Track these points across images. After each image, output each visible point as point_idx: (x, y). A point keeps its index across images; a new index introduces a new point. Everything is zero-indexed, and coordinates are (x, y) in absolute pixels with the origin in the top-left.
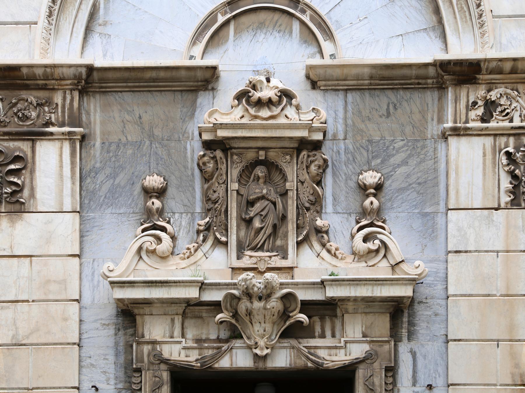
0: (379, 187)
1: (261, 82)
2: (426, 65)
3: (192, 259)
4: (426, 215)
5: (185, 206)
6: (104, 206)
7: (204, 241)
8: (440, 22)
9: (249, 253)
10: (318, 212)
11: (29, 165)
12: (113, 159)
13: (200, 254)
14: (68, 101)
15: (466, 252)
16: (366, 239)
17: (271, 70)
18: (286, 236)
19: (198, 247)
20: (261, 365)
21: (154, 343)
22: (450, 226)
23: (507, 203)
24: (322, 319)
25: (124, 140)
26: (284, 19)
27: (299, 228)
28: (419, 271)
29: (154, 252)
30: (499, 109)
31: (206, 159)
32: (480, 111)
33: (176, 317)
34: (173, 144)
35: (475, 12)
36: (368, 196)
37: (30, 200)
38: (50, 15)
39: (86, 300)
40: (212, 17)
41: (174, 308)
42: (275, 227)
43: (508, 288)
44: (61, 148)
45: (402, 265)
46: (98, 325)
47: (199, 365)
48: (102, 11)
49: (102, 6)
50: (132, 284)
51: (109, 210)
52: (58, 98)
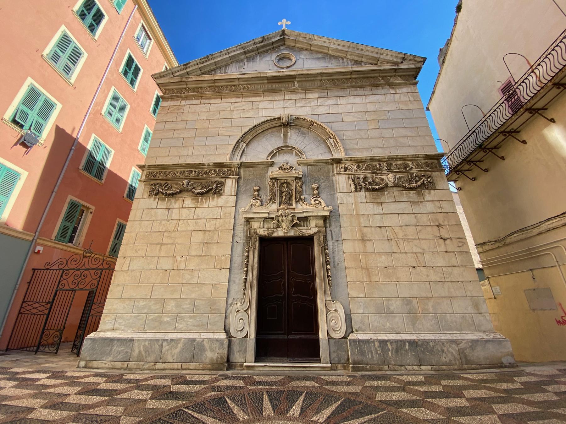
0: (318, 188)
8: (331, 150)
13: (268, 205)
16: (315, 201)
18: (292, 200)
20: (286, 235)
21: (255, 229)
24: (304, 222)
27: (296, 199)
40: (273, 151)
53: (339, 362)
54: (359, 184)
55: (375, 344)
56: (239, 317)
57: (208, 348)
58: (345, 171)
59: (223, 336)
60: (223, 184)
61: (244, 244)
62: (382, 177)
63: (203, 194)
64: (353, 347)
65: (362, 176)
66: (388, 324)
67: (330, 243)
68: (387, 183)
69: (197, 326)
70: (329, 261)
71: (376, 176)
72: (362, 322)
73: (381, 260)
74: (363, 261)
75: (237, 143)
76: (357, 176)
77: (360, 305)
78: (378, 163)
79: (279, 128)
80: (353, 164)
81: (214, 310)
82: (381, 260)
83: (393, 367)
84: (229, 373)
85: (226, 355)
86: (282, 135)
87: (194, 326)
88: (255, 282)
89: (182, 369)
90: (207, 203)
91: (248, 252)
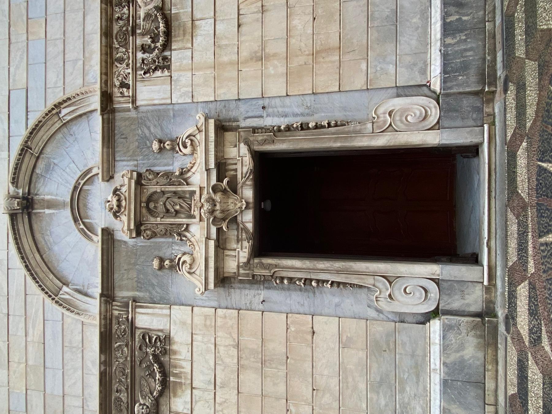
0: (160, 142)
1: (109, 205)
2: (103, 119)
3: (195, 243)
4: (174, 116)
5: (168, 247)
6: (168, 292)
7: (186, 237)
8: (85, 114)
9: (192, 212)
10: (172, 174)
11: (147, 331)
12: (145, 285)
13: (192, 239)
14: (117, 308)
15: (192, 92)
16: (185, 147)
17: (105, 200)
18: (184, 192)
19: (189, 240)
20: (251, 205)
21: (238, 267)
22: (180, 102)
23: (168, 72)
24: (227, 171)
25: (136, 279)
26: (82, 194)
27: (180, 184)
28: (201, 117)
29: (191, 265)
30: (124, 80)
31: (145, 235)
32: (125, 90)
33: (225, 254)
34: (139, 253)
35: (81, 97)
36: (164, 147)
37: (164, 332)
38: (78, 314)
39: (215, 304)
40: (82, 231)
41: (220, 255)
42: (179, 198)
43: (211, 67)
44: (139, 313)
45: (199, 127)
46: (229, 298)
47: (251, 241)
48: (78, 287)
49: (75, 287)
50: (206, 279)
51: (170, 289)
52: (116, 313)
53: (480, 110)
54: (155, 61)
55: (450, 44)
56: (402, 296)
57: (458, 355)
58: (127, 86)
59: (436, 325)
60: (146, 334)
61: (267, 288)
62: (142, 16)
63: (165, 374)
64: (454, 83)
65: (140, 55)
66: (414, 20)
67: (269, 122)
68: (155, 7)
69: (418, 376)
70: (301, 124)
71: (140, 29)
72: (411, 67)
73: (300, 27)
74: (301, 60)
75: (61, 305)
76: (138, 65)
77: (382, 69)
78: (114, 24)
79: (33, 217)
80: (115, 70)
81: (388, 345)
82: (300, 27)
83: (489, 13)
84: (501, 313)
85: (471, 319)
86: (47, 211)
87: (417, 383)
88: (338, 264)
89: (496, 404)
90: (184, 364)
91: (282, 279)
